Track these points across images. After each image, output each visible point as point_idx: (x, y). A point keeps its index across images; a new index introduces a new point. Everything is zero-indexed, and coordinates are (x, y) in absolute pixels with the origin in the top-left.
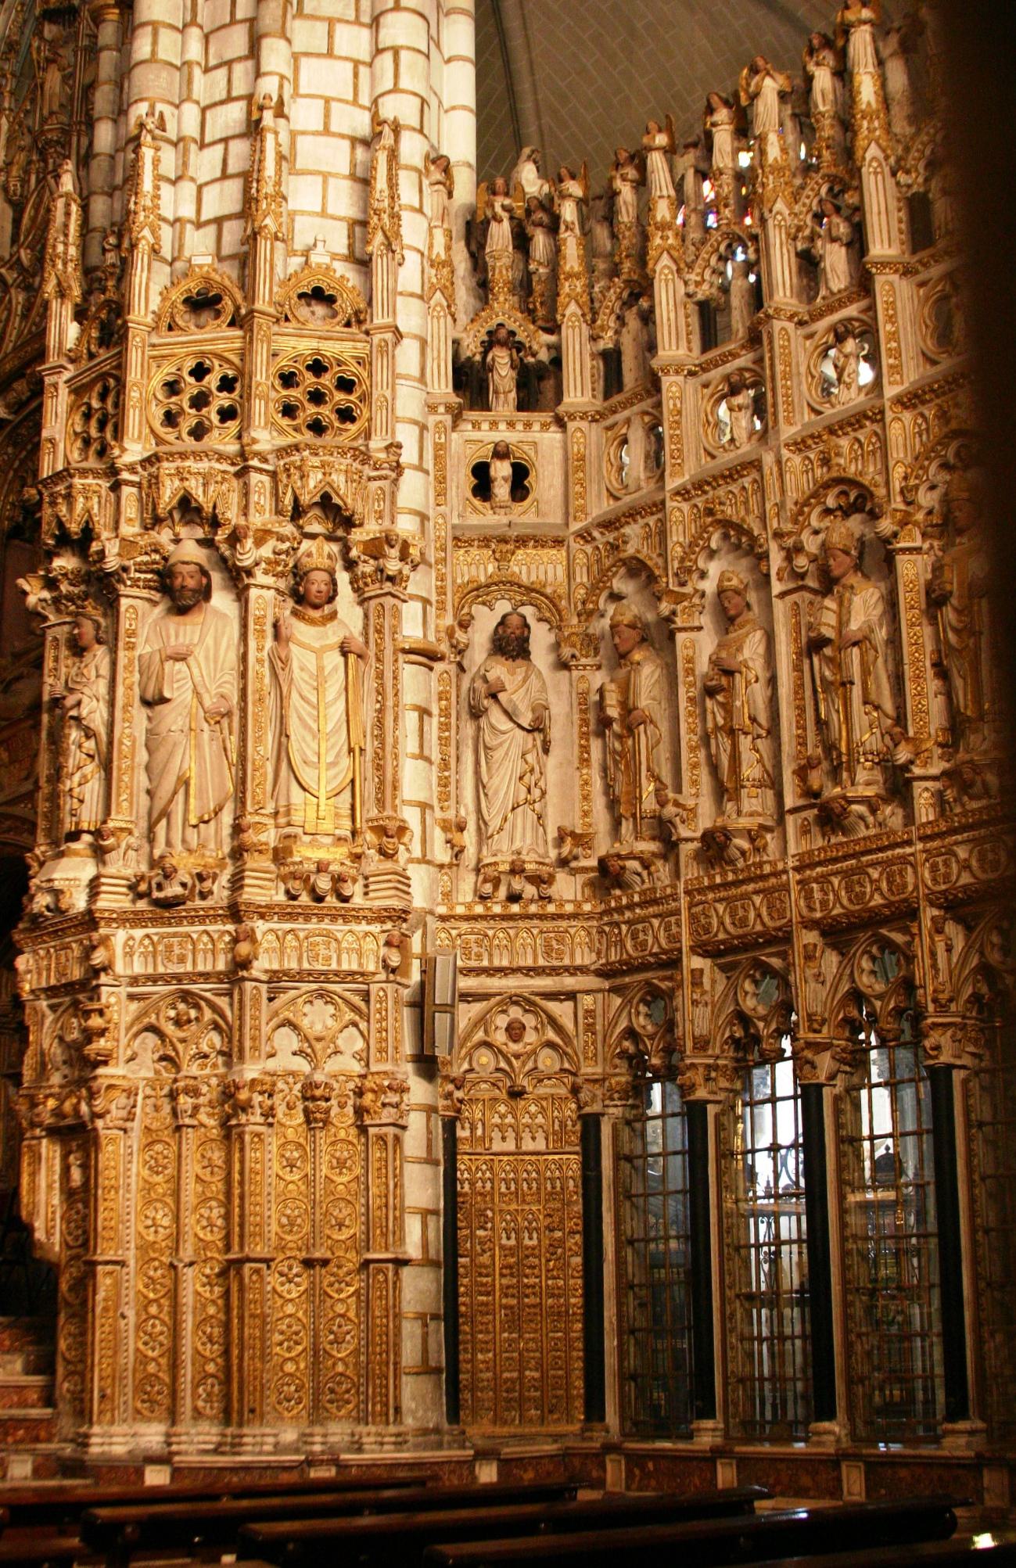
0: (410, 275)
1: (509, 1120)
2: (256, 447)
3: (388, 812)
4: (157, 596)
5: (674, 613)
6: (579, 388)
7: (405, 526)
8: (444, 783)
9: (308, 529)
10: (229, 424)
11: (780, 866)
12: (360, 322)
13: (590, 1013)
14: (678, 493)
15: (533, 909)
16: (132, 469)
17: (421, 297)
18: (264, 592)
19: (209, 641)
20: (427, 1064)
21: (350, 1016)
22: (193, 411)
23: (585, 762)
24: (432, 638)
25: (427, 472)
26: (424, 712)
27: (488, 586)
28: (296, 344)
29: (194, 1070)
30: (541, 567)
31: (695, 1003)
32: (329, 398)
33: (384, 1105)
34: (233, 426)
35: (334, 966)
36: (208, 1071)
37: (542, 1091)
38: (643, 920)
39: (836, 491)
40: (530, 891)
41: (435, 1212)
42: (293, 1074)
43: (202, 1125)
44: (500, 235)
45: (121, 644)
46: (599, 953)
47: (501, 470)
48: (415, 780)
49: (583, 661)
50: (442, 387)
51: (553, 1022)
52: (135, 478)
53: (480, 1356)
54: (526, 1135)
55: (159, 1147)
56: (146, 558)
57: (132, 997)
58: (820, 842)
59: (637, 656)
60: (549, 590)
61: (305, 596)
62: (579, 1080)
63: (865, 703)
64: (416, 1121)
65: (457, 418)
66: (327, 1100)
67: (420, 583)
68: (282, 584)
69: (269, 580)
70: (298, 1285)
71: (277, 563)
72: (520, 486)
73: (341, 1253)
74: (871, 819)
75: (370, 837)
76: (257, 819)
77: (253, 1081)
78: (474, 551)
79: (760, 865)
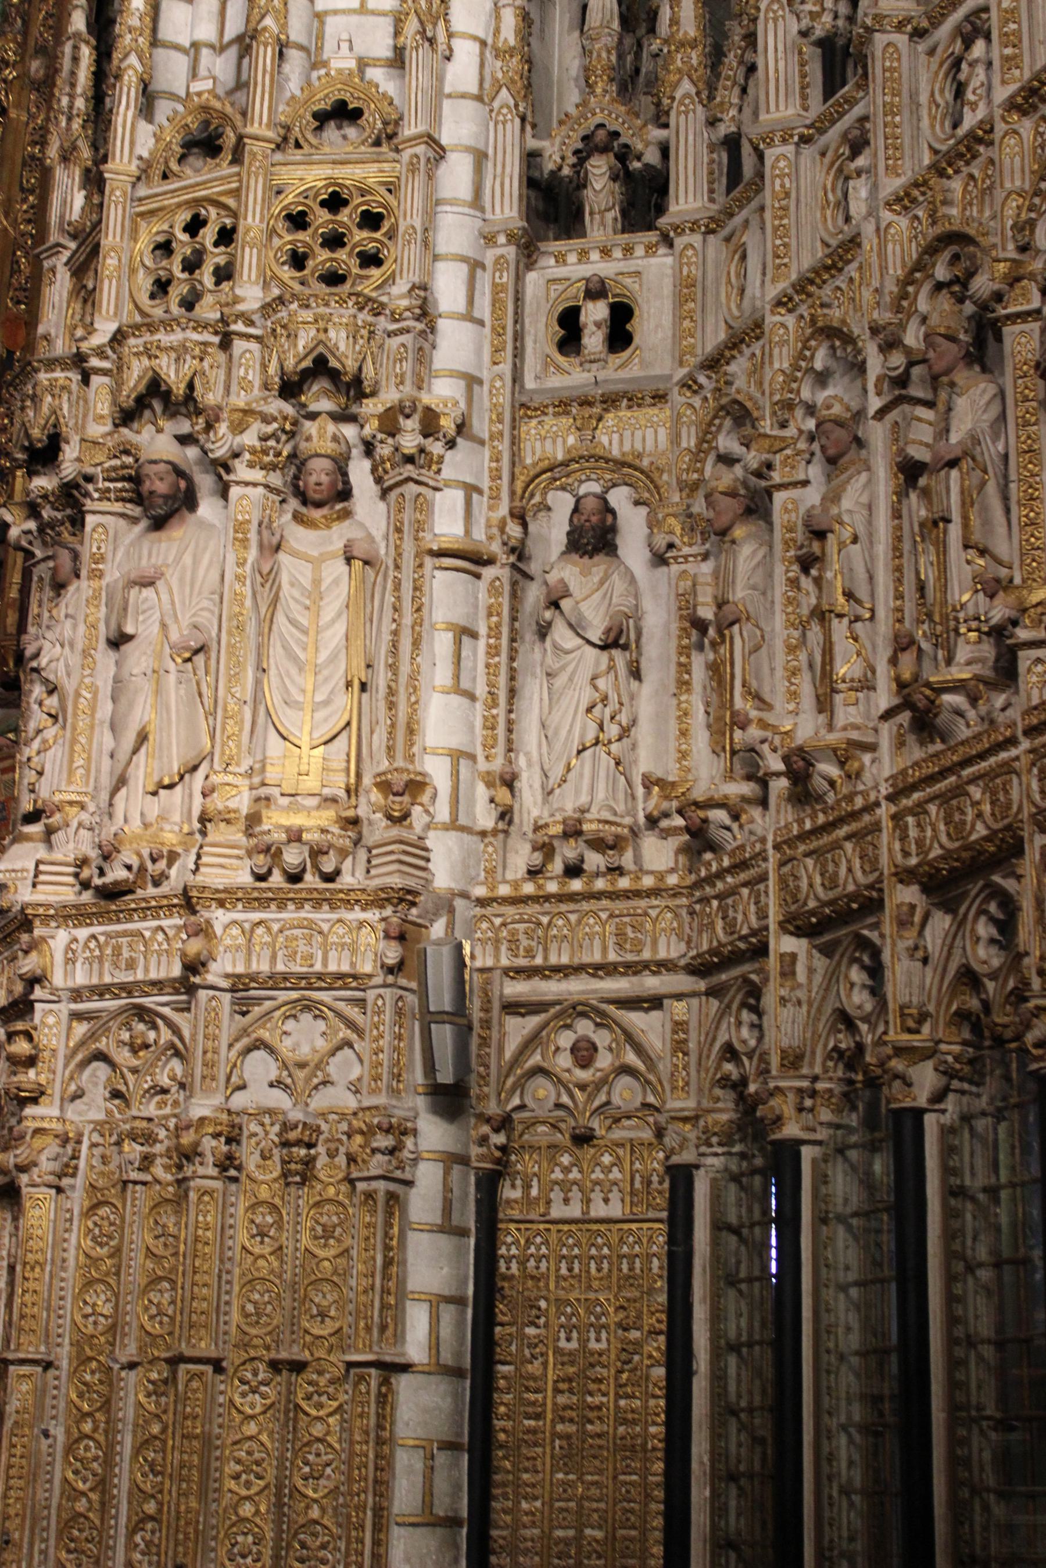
1: (575, 1174)
2: (241, 307)
3: (400, 763)
5: (769, 466)
7: (443, 392)
8: (490, 725)
9: (313, 407)
11: (872, 797)
12: (390, 137)
13: (679, 1026)
14: (779, 303)
15: (600, 884)
16: (100, 353)
17: (479, 98)
18: (250, 490)
19: (187, 559)
21: (345, 1033)
22: (185, 276)
23: (684, 685)
24: (479, 534)
25: (481, 323)
26: (464, 632)
27: (565, 464)
28: (306, 177)
29: (151, 1109)
30: (639, 434)
31: (783, 1001)
32: (344, 240)
33: (374, 1151)
35: (318, 967)
36: (168, 1110)
37: (617, 1134)
38: (733, 892)
39: (946, 255)
40: (594, 860)
41: (458, 1301)
42: (270, 1112)
43: (158, 1181)
46: (688, 943)
48: (444, 723)
49: (686, 550)
50: (507, 208)
51: (630, 1038)
52: (106, 365)
53: (524, 1505)
54: (597, 1196)
56: (116, 462)
57: (77, 1016)
58: (918, 753)
59: (738, 532)
60: (645, 463)
62: (662, 1119)
63: (966, 547)
64: (428, 1177)
66: (310, 1146)
68: (276, 479)
69: (257, 475)
70: (264, 1396)
71: (265, 452)
72: (619, 337)
73: (321, 1353)
74: (971, 714)
75: (376, 796)
76: (230, 778)
77: (202, 1119)
78: (549, 420)
79: (850, 798)
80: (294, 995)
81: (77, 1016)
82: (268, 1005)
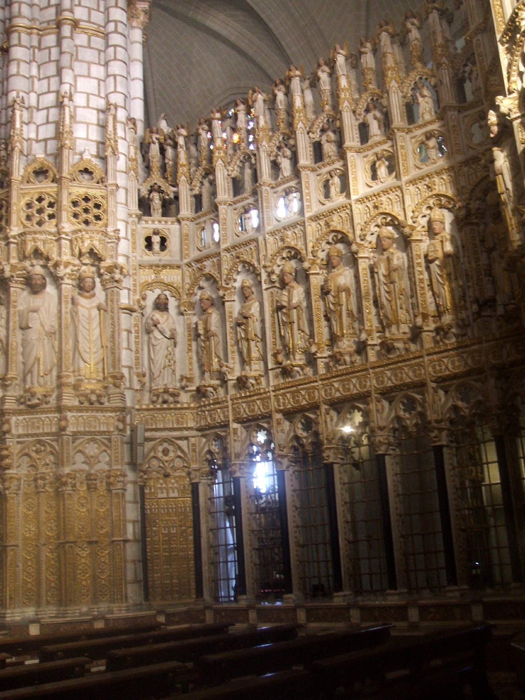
0: (122, 164)
1: (164, 486)
2: (64, 230)
4: (24, 287)
6: (186, 209)
7: (121, 261)
8: (137, 359)
10: (52, 220)
12: (103, 182)
13: (194, 445)
15: (172, 406)
17: (126, 173)
19: (46, 305)
20: (133, 465)
21: (103, 448)
24: (132, 304)
25: (128, 240)
26: (129, 332)
29: (44, 470)
30: (172, 277)
31: (235, 440)
32: (91, 211)
33: (118, 482)
34: (54, 221)
35: (98, 429)
36: (49, 470)
37: (176, 474)
40: (171, 399)
41: (137, 521)
42: (82, 471)
43: (48, 491)
44: (155, 149)
45: (11, 306)
46: (197, 422)
47: (156, 239)
49: (189, 312)
51: (180, 448)
52: (15, 241)
53: (155, 575)
54: (171, 491)
55: (30, 500)
56: (20, 272)
57: (18, 442)
61: (83, 287)
62: (190, 470)
64: (130, 488)
65: (139, 218)
66: (96, 480)
67: (127, 282)
68: (74, 283)
69: (70, 281)
71: (73, 275)
73: (102, 538)
75: (110, 380)
76: (67, 373)
77: (68, 474)
78: (147, 270)
80: (90, 437)
81: (18, 442)
82: (81, 440)
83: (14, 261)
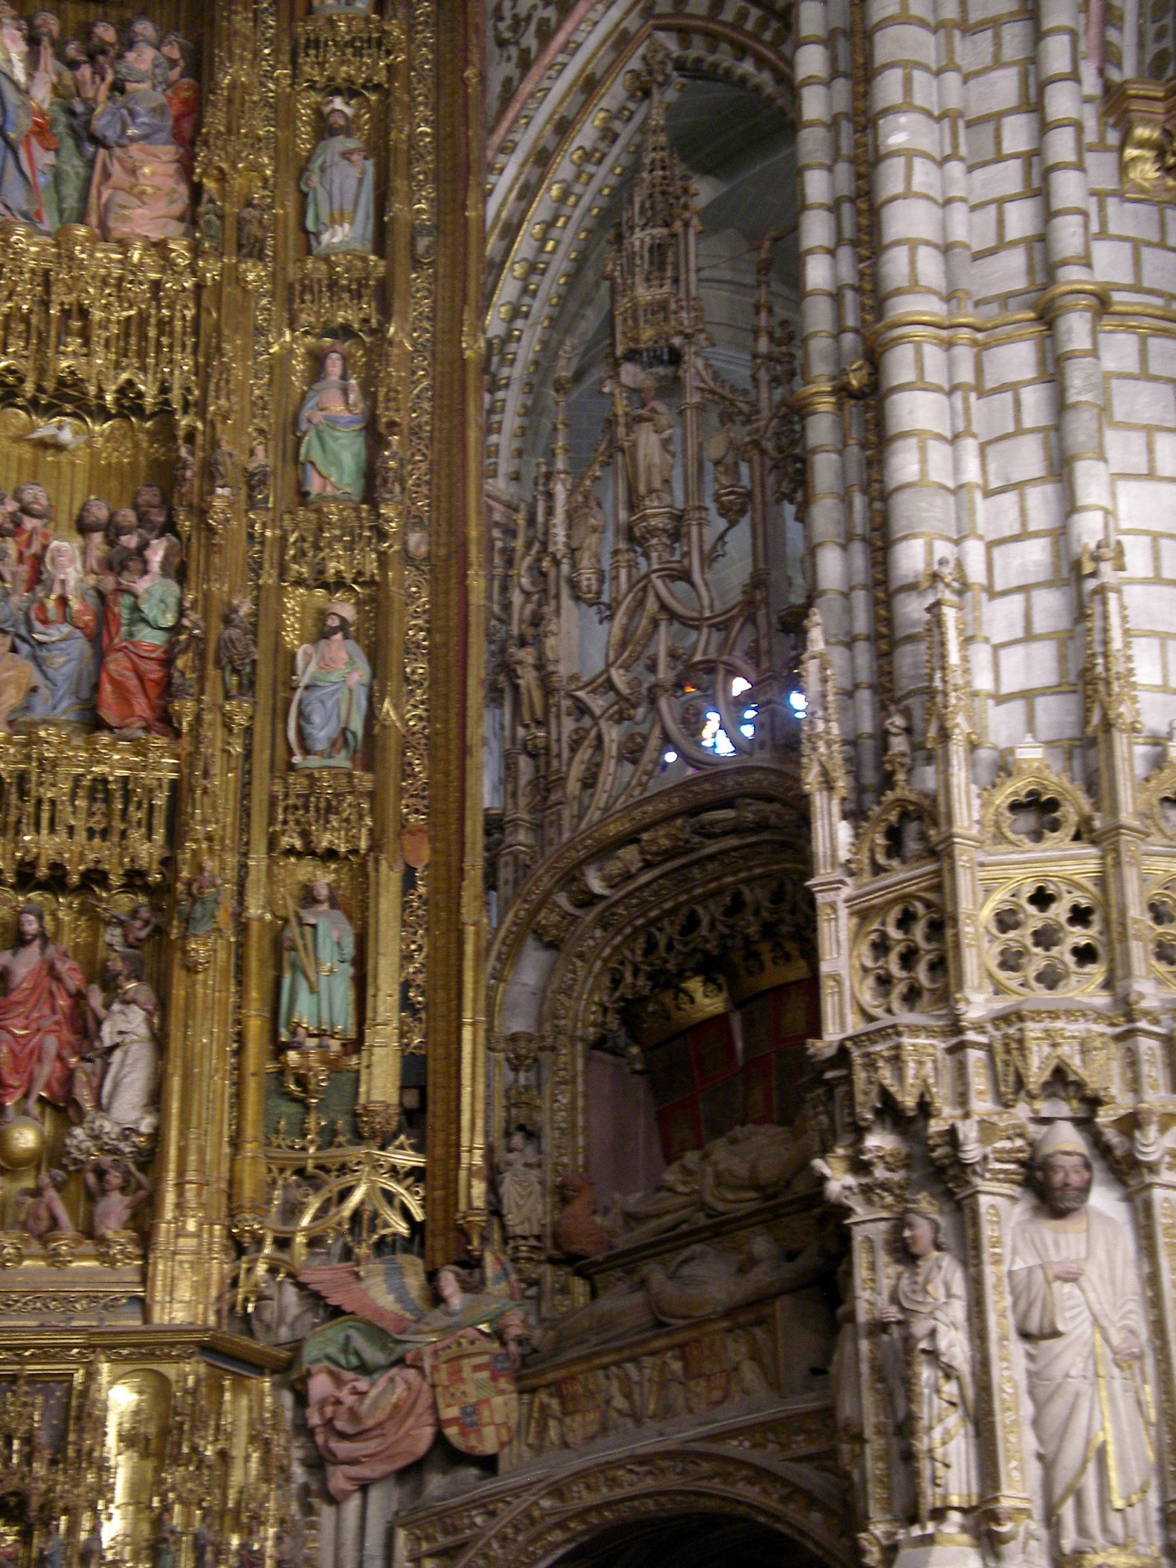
2: (1145, 1004)
4: (1016, 1191)
10: (1089, 968)
16: (979, 1028)
19: (1100, 1254)
22: (1038, 950)
34: (1097, 971)
45: (986, 1257)
52: (982, 1039)
56: (1007, 1144)
83: (982, 1105)
